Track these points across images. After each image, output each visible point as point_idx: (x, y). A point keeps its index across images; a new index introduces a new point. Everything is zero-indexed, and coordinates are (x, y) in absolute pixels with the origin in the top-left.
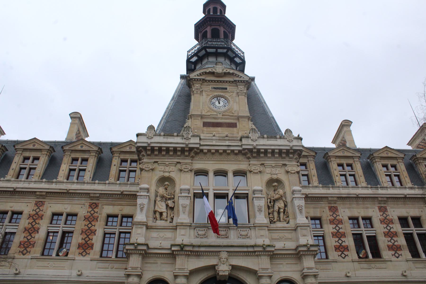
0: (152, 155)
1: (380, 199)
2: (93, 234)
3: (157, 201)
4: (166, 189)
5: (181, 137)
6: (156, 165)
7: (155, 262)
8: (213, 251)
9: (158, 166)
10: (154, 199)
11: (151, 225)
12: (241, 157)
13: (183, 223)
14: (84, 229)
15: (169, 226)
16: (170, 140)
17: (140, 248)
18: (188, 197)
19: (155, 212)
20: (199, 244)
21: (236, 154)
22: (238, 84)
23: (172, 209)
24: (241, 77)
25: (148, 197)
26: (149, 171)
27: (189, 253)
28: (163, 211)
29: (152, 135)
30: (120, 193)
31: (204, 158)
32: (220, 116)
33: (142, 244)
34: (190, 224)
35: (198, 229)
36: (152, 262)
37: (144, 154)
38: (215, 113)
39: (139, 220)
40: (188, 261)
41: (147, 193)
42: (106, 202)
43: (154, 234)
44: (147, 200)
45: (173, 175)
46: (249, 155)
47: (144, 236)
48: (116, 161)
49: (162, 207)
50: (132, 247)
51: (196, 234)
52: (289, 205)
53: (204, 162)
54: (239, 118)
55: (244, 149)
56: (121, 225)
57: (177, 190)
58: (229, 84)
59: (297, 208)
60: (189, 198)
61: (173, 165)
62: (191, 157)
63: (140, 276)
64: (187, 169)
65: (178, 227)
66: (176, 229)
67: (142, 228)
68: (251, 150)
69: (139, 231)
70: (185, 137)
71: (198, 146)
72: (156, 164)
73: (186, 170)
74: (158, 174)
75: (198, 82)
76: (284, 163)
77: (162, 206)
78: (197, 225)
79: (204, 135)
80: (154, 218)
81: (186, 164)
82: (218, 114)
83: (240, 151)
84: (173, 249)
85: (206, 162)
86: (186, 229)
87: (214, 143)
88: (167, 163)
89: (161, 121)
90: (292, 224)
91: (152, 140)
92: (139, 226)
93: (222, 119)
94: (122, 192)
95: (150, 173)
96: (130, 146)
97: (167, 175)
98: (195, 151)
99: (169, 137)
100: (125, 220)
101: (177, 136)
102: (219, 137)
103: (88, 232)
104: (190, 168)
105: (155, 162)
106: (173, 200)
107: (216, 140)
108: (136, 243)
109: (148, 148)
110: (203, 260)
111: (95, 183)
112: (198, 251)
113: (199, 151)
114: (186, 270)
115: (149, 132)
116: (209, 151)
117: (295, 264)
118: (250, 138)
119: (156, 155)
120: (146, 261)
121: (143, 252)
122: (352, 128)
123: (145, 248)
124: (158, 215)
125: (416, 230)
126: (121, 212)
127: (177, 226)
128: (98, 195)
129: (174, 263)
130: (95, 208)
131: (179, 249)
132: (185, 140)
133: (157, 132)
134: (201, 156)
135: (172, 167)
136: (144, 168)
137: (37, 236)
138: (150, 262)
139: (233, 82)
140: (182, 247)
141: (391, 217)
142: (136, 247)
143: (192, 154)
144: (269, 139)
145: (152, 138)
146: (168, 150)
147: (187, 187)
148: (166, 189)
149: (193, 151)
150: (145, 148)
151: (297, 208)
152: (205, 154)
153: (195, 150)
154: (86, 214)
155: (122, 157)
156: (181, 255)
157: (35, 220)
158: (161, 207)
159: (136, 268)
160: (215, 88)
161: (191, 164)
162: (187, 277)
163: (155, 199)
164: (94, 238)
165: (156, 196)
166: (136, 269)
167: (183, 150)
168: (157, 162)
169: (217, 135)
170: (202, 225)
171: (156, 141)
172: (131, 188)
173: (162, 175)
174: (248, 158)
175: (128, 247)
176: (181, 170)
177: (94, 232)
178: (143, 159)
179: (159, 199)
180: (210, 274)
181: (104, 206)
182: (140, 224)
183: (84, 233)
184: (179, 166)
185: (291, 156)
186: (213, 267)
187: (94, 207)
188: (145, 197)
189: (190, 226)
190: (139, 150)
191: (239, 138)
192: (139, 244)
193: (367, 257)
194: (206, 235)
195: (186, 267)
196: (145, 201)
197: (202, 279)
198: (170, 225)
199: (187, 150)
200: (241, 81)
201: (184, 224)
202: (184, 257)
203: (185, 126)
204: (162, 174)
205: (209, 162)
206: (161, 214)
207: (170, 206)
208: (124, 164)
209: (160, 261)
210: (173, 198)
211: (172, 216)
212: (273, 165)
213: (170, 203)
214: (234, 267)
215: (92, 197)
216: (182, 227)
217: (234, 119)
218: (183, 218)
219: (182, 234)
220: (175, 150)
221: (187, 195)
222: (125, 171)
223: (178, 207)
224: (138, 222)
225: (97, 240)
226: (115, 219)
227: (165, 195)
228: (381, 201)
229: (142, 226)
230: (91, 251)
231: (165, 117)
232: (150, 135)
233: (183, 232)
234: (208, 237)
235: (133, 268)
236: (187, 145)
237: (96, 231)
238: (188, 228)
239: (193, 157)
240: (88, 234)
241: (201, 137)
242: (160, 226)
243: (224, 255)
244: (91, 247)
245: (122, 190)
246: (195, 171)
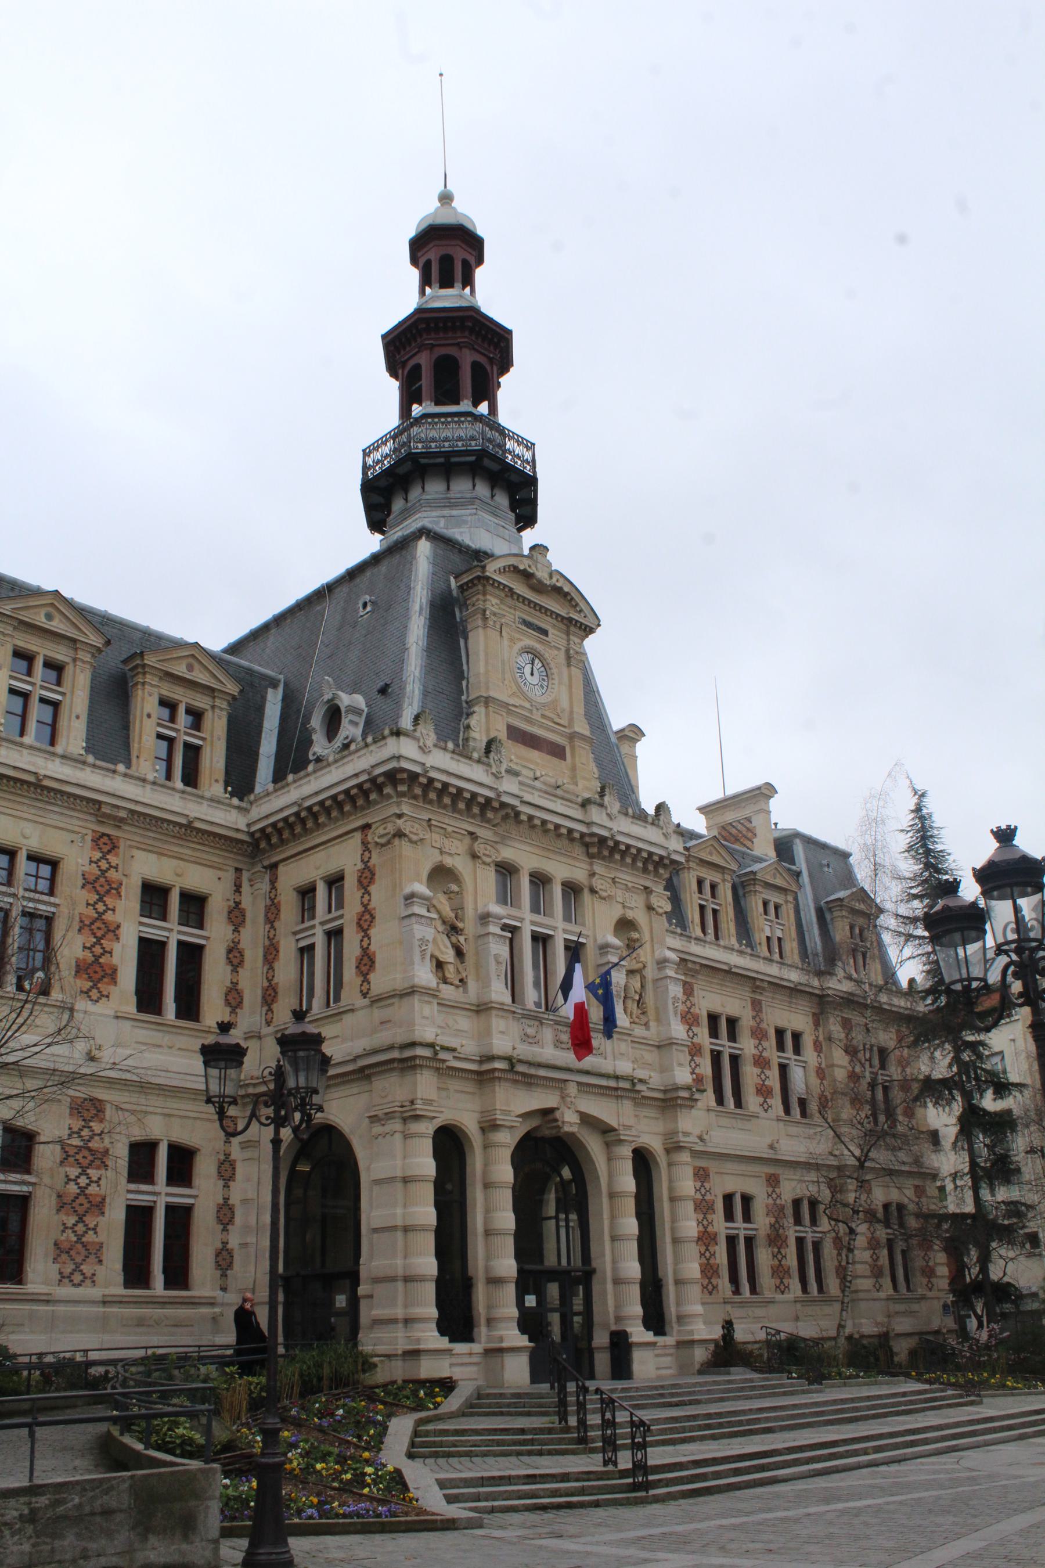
1: (690, 965)
2: (110, 935)
5: (485, 767)
12: (578, 850)
14: (87, 916)
21: (572, 840)
22: (572, 628)
24: (581, 611)
30: (184, 821)
32: (536, 716)
38: (527, 705)
42: (138, 839)
46: (594, 850)
50: (426, 1052)
52: (649, 986)
54: (572, 737)
55: (593, 835)
58: (555, 622)
59: (670, 1002)
64: (489, 856)
67: (429, 1003)
68: (602, 840)
70: (494, 771)
75: (497, 592)
76: (648, 884)
82: (535, 711)
83: (583, 835)
90: (653, 1033)
93: (541, 726)
103: (99, 928)
107: (540, 790)
111: (114, 772)
112: (531, 1076)
117: (656, 1118)
118: (606, 808)
125: (730, 1047)
126: (179, 879)
128: (123, 814)
130: (109, 852)
136: (407, 832)
139: (563, 618)
141: (698, 1011)
144: (635, 821)
151: (670, 1002)
154: (87, 868)
156: (506, 1080)
158: (444, 949)
160: (526, 623)
164: (117, 948)
166: (431, 1105)
173: (439, 858)
174: (591, 856)
177: (113, 931)
181: (136, 853)
183: (86, 930)
185: (661, 871)
186: (547, 1113)
187: (106, 848)
188: (429, 921)
191: (580, 800)
200: (582, 624)
212: (630, 885)
215: (105, 815)
216: (500, 1013)
217: (562, 735)
225: (125, 958)
228: (691, 970)
229: (431, 999)
230: (112, 988)
237: (118, 927)
240: (99, 934)
243: (572, 1089)
244: (111, 974)
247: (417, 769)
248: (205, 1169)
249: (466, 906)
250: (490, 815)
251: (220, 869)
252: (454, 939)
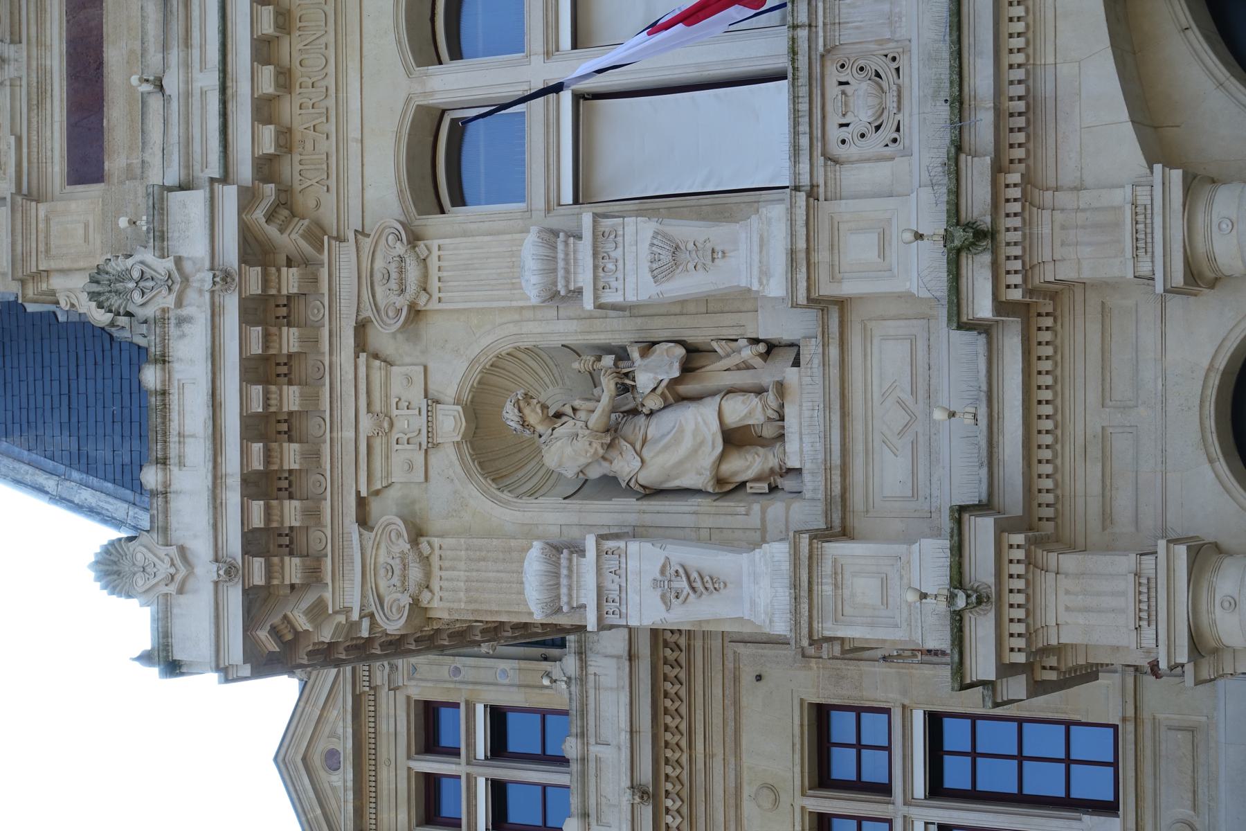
0: (315, 547)
3: (649, 476)
4: (558, 415)
5: (173, 331)
6: (385, 513)
7: (1095, 451)
9: (393, 493)
10: (632, 502)
11: (820, 507)
13: (792, 253)
15: (825, 363)
16: (190, 413)
17: (981, 568)
18: (598, 237)
19: (727, 488)
20: (944, 111)
23: (694, 357)
25: (610, 544)
26: (425, 561)
27: (1015, 178)
28: (715, 426)
29: (162, 551)
30: (647, 812)
31: (323, 146)
33: (958, 550)
34: (802, 196)
35: (834, 134)
36: (1095, 471)
37: (309, 599)
39: (784, 596)
40: (1078, 188)
41: (582, 552)
43: (887, 474)
44: (634, 546)
45: (452, 376)
47: (900, 549)
49: (684, 441)
50: (982, 629)
51: (875, 143)
53: (354, 148)
56: (884, 790)
57: (560, 329)
60: (607, 223)
61: (377, 377)
62: (320, 249)
63: (1204, 555)
65: (826, 289)
66: (842, 303)
69: (863, 589)
70: (170, 301)
71: (229, 196)
72: (375, 506)
73: (413, 273)
74: (451, 490)
77: (681, 431)
78: (804, 141)
79: (155, 160)
80: (773, 489)
81: (367, 279)
84: (983, 308)
85: (354, 133)
86: (834, 228)
87: (210, 80)
88: (366, 423)
89: (78, 508)
91: (201, 548)
92: (826, 589)
94: (644, 794)
96: (317, 760)
97: (451, 423)
98: (269, 218)
99: (174, 426)
100: (843, 765)
101: (163, 360)
102: (165, 48)
104: (400, 249)
105: (363, 521)
106: (635, 354)
108: (951, 598)
109: (258, 579)
110: (1064, 70)
113: (270, 189)
114: (1143, 199)
115: (140, 580)
116: (264, 110)
119: (313, 514)
120: (1094, 522)
121: (1019, 539)
123: (982, 530)
124: (747, 465)
126: (785, 799)
127: (818, 303)
131: (987, 258)
132: (191, 295)
133: (145, 520)
135: (397, 387)
136: (406, 600)
138: (1095, 488)
140: (967, 237)
142: (979, 601)
143: (290, 240)
145: (182, 550)
146: (264, 427)
147: (530, 248)
148: (558, 415)
149: (272, 231)
150: (257, 602)
152: (286, 139)
153: (259, 215)
155: (403, 816)
156: (1028, 242)
158: (687, 444)
159: (1144, 587)
161: (366, 243)
162: (1198, 183)
163: (629, 491)
165: (610, 485)
167: (263, 311)
168: (361, 502)
169: (154, 58)
170: (804, 107)
171: (202, 521)
172: (607, 732)
175: (983, 665)
176: (415, 313)
178: (347, 611)
182: (804, 585)
184: (383, 336)
189: (812, 194)
190: (273, 647)
192: (958, 579)
194: (874, 64)
195: (1121, 197)
196: (643, 560)
197: (1221, 72)
198: (817, 361)
199: (266, 282)
201: (801, 244)
202: (1044, 224)
203: (101, 318)
204: (448, 460)
205: (354, 104)
206: (735, 439)
207: (677, 374)
209: (1085, 413)
210: (621, 354)
211: (748, 353)
213: (650, 375)
216: (822, 256)
218: (753, 261)
219: (872, 255)
220: (263, 369)
221: (585, 247)
222: (499, 790)
223: (682, 306)
224: (796, 599)
227: (595, 420)
229: (828, 568)
231: (50, 483)
232: (164, 569)
233: (859, 249)
234: (890, 48)
235: (1145, 615)
236: (224, 278)
238: (825, 209)
239: (317, 234)
241: (172, 179)
242: (826, 436)
245: (626, 798)
246: (422, 212)
247: (234, 599)
249: (557, 341)
250: (290, 281)
251: (736, 680)
252: (653, 403)
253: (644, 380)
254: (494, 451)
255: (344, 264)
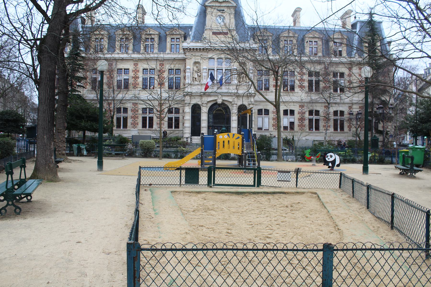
8: (216, 94)
19: (193, 77)
23: (200, 76)
45: (199, 60)
48: (169, 39)
71: (210, 47)
74: (193, 60)
95: (190, 60)
122: (301, 13)
124: (194, 79)
129: (201, 99)
134: (211, 51)
137: (139, 80)
143: (208, 51)
157: (136, 73)
165: (193, 70)
167: (203, 49)
179: (194, 72)
180: (215, 102)
186: (216, 100)
193: (287, 90)
208: (173, 40)
214: (223, 100)
226: (173, 71)
248: (181, 111)
253: (199, 74)
254: (196, 63)
255: (206, 54)
